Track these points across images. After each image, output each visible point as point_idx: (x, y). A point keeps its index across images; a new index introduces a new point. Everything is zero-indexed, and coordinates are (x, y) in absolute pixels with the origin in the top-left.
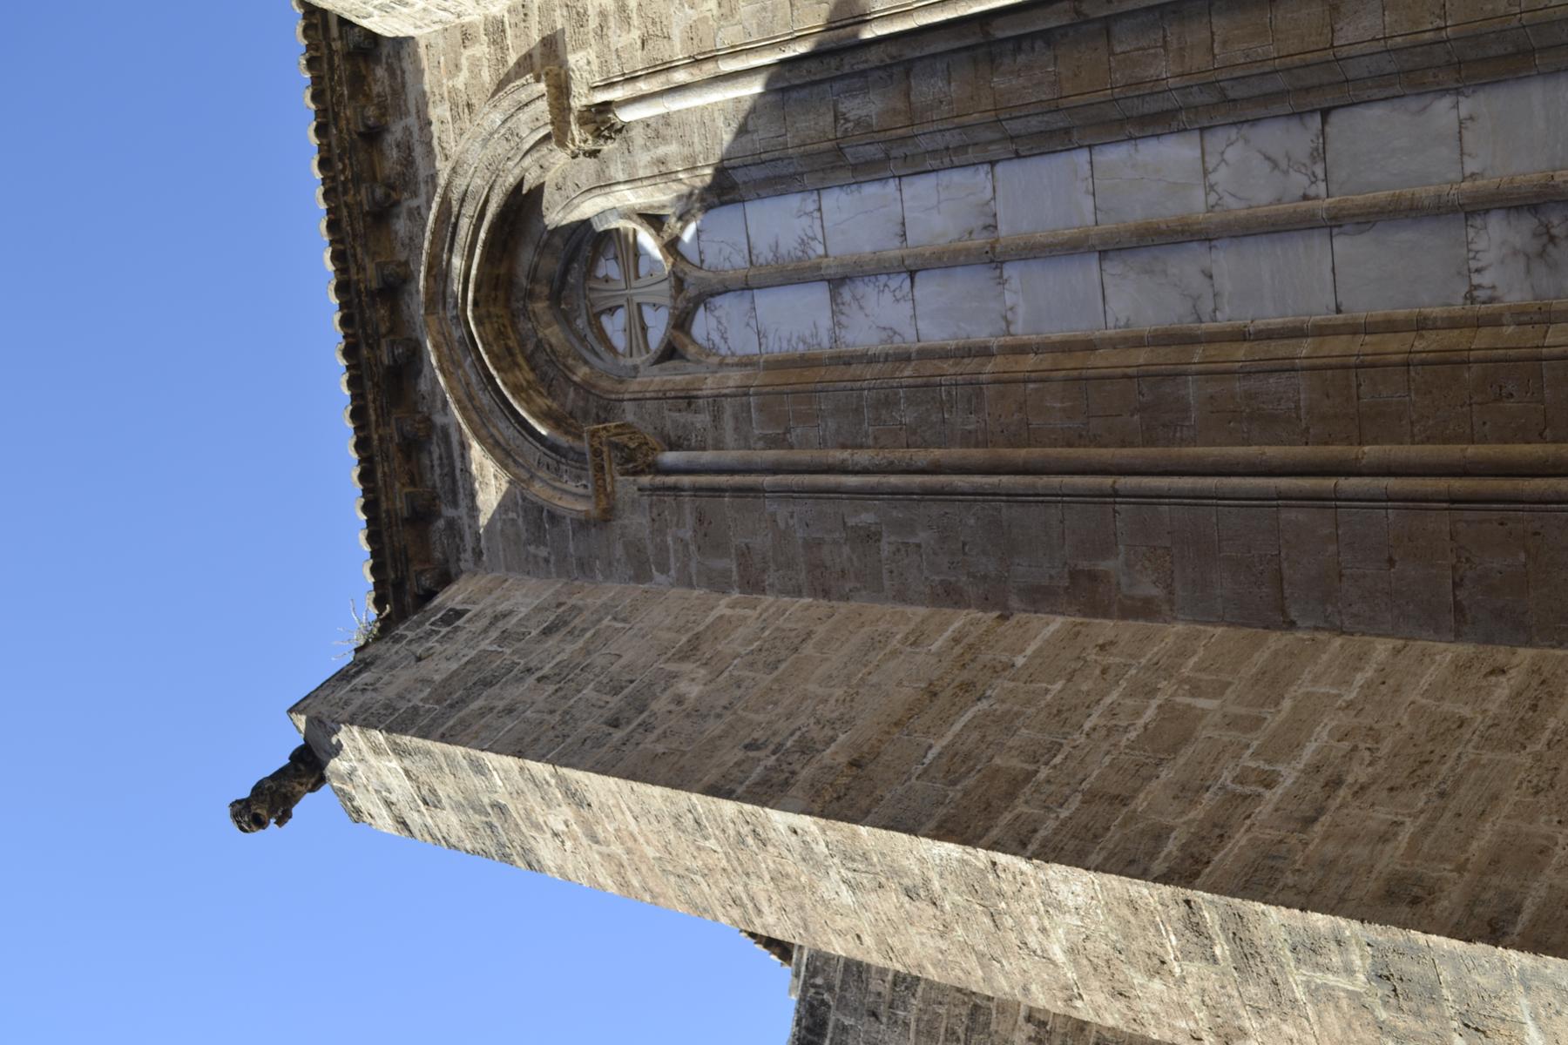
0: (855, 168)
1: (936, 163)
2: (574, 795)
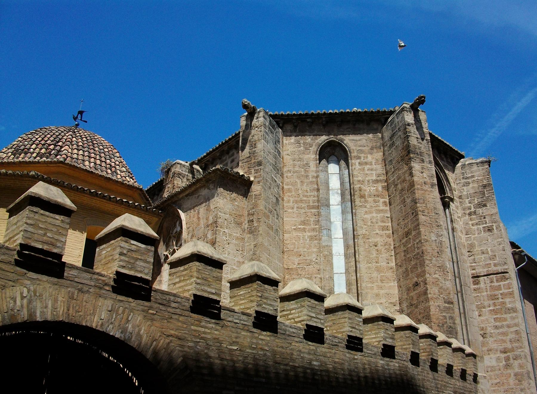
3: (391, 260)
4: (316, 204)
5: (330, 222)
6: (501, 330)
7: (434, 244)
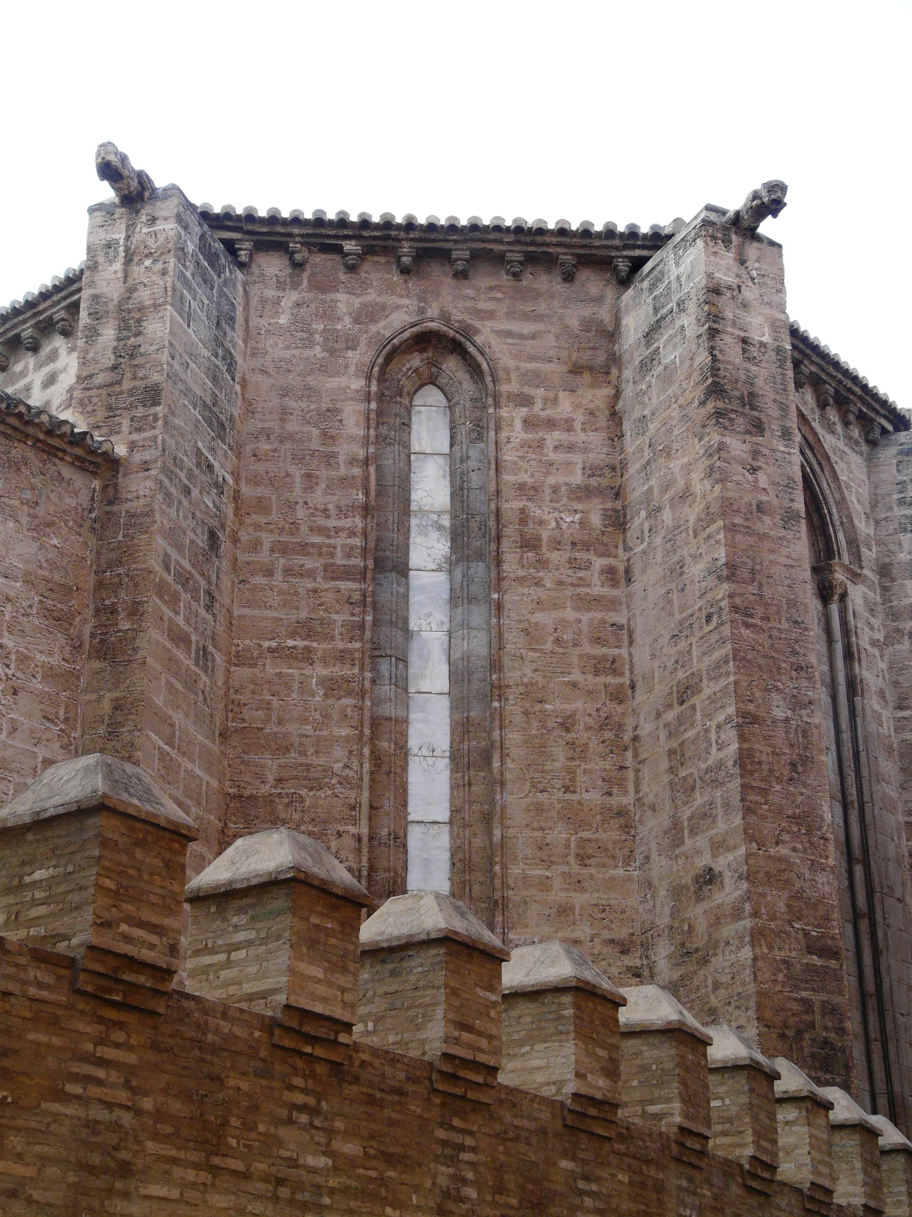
3: (621, 784)
4: (358, 562)
5: (406, 631)
7: (780, 733)
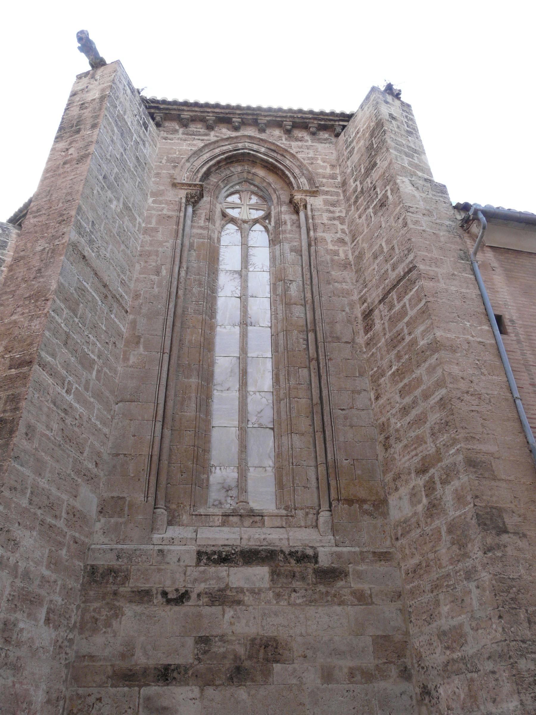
0: (275, 284)
1: (273, 310)
2: (82, 159)
6: (414, 413)
